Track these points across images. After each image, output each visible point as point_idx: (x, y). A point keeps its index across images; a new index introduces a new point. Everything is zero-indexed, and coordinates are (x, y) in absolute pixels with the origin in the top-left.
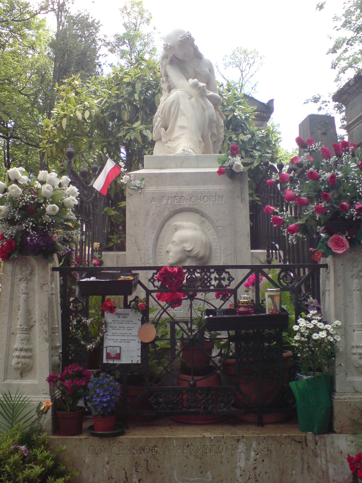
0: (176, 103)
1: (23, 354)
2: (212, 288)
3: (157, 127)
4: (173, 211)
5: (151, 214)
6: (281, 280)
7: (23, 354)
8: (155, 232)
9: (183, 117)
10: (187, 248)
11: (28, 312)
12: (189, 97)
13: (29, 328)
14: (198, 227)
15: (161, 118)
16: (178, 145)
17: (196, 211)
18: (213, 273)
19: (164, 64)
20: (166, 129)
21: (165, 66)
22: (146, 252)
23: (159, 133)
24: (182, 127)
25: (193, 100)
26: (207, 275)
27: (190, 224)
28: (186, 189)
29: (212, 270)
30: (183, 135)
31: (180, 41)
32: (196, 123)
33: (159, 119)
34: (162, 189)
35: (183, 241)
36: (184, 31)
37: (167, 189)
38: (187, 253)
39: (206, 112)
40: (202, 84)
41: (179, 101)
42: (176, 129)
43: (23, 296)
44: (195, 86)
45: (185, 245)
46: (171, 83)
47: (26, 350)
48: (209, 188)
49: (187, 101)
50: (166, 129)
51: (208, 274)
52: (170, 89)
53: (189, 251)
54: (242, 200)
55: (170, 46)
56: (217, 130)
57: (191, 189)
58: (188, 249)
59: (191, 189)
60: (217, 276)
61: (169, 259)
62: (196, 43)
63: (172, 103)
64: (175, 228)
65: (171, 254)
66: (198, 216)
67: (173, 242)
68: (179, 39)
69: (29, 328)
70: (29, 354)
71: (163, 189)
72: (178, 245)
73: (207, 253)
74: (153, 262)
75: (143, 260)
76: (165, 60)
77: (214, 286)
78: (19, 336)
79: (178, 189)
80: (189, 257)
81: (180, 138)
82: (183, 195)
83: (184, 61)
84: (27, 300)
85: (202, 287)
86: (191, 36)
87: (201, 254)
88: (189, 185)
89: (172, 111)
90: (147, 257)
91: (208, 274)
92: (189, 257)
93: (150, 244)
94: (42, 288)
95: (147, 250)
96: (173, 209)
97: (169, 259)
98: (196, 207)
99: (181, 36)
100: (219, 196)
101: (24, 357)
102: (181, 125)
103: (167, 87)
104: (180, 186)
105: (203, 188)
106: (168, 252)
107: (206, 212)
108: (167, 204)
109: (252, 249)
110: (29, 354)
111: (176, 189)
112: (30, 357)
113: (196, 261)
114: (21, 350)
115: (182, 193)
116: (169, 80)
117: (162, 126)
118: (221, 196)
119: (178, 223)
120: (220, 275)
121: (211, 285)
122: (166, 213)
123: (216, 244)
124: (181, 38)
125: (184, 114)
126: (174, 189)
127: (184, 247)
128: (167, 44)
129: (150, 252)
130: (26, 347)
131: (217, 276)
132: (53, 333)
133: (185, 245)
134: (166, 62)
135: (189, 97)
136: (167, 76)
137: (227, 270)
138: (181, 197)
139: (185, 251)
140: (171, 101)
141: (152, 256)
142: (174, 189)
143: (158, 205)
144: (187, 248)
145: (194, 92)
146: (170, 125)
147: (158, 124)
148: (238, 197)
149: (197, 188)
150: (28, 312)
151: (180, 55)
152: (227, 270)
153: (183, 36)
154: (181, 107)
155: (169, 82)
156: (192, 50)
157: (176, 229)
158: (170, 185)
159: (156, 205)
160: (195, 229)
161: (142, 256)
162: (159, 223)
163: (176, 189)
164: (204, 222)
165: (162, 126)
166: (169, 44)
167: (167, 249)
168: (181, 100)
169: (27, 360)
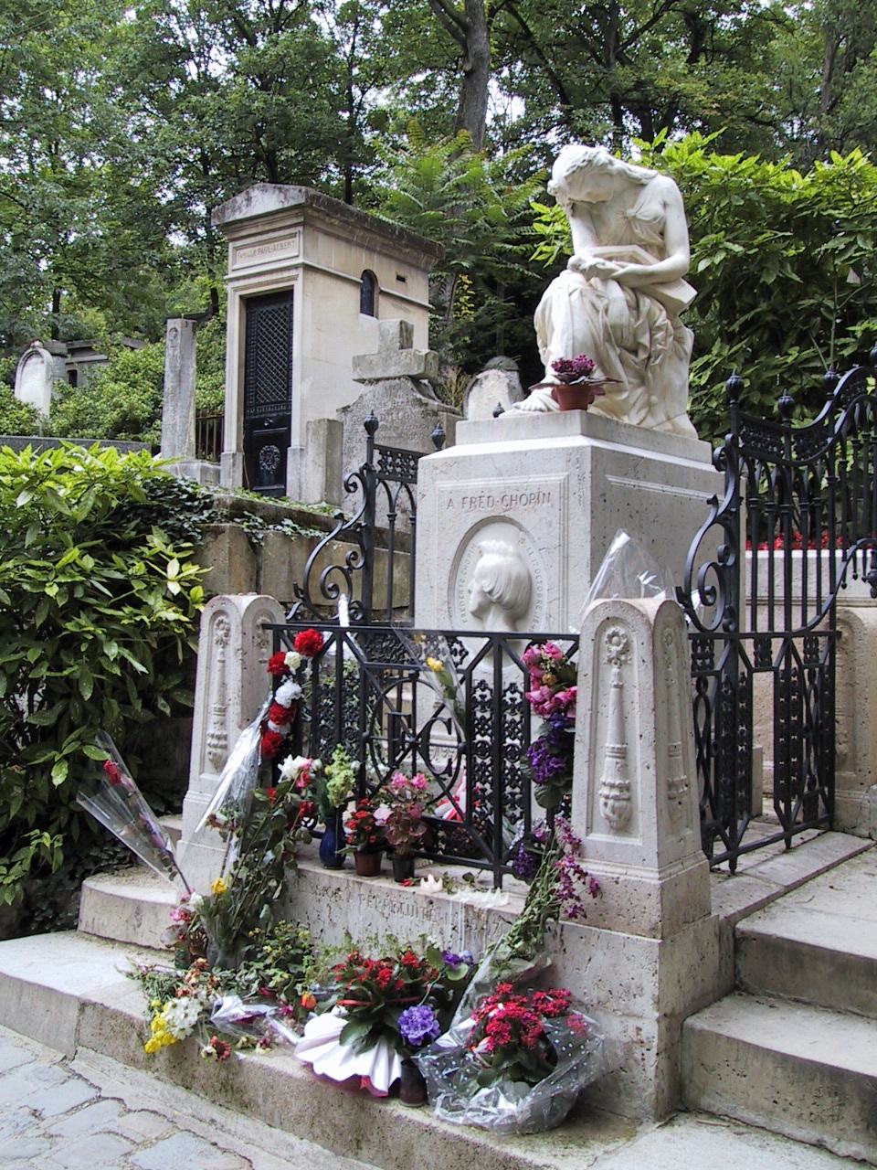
1: (215, 742)
7: (215, 742)
11: (223, 685)
13: (223, 711)
14: (511, 549)
17: (511, 521)
27: (501, 544)
32: (571, 342)
34: (463, 484)
35: (482, 576)
43: (219, 665)
47: (219, 738)
53: (490, 592)
56: (651, 337)
58: (487, 590)
65: (472, 596)
66: (515, 529)
69: (223, 711)
70: (222, 742)
78: (214, 718)
80: (492, 602)
84: (223, 670)
87: (507, 598)
88: (502, 475)
98: (509, 514)
101: (215, 746)
106: (470, 592)
107: (524, 524)
110: (222, 742)
112: (225, 747)
114: (213, 736)
123: (539, 580)
130: (218, 733)
133: (484, 581)
137: (459, 639)
150: (223, 685)
152: (459, 639)
157: (481, 554)
158: (477, 477)
160: (505, 553)
167: (469, 587)
169: (219, 751)
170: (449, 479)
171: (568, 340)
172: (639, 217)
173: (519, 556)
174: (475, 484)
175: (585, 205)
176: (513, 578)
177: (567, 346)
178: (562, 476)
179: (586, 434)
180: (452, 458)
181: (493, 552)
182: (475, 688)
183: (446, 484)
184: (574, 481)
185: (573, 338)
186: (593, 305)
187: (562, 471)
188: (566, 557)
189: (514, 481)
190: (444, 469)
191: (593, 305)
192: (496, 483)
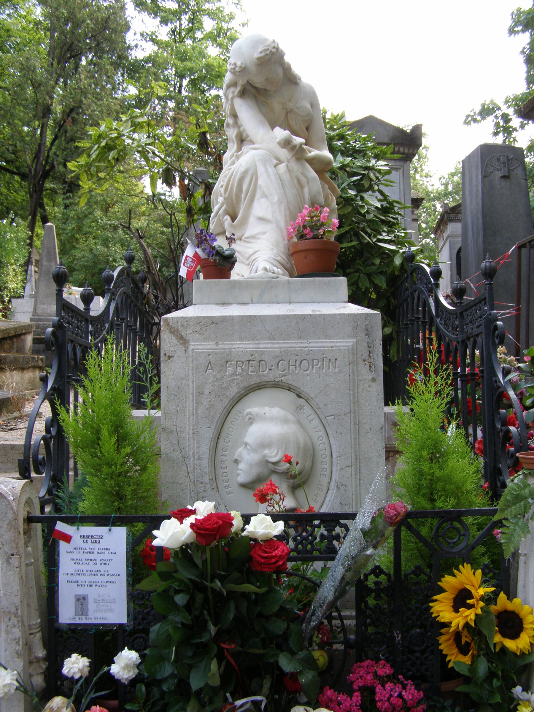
0: (250, 175)
2: (316, 553)
3: (217, 213)
4: (244, 388)
5: (206, 392)
6: (441, 538)
8: (213, 426)
9: (263, 200)
10: (271, 457)
12: (275, 162)
14: (290, 417)
15: (225, 199)
16: (255, 252)
18: (319, 526)
19: (230, 96)
20: (233, 219)
21: (232, 99)
22: (197, 462)
23: (221, 224)
24: (261, 219)
25: (282, 167)
26: (306, 531)
27: (276, 411)
28: (269, 346)
29: (316, 522)
30: (264, 233)
31: (258, 59)
32: (288, 212)
33: (221, 199)
34: (226, 345)
35: (263, 445)
36: (266, 40)
37: (234, 346)
38: (271, 466)
39: (306, 190)
40: (298, 140)
41: (256, 170)
42: (252, 220)
44: (286, 144)
45: (266, 452)
46: (242, 129)
48: (311, 345)
49: (271, 170)
50: (233, 219)
51: (309, 529)
52: (242, 140)
54: (370, 367)
55: (240, 67)
57: (278, 346)
58: (274, 460)
59: (278, 346)
60: (326, 533)
61: (238, 475)
62: (287, 59)
63: (245, 173)
64: (250, 418)
65: (242, 466)
66: (292, 396)
67: (246, 444)
68: (257, 55)
71: (227, 347)
72: (254, 450)
73: (308, 464)
74: (210, 479)
75: (192, 477)
76: (232, 89)
77: (319, 550)
79: (255, 346)
81: (259, 239)
82: (263, 358)
83: (266, 90)
85: (299, 552)
86: (277, 49)
88: (274, 339)
89: (245, 187)
90: (199, 471)
91: (309, 529)
92: (274, 472)
93: (205, 448)
94: (8, 561)
95: (199, 459)
96: (245, 384)
97: (238, 475)
99: (261, 49)
100: (330, 360)
102: (261, 215)
103: (236, 137)
104: (258, 340)
105: (301, 345)
106: (236, 462)
107: (306, 390)
108: (234, 374)
109: (386, 404)
111: (251, 346)
113: (288, 479)
115: (262, 353)
116: (239, 123)
117: (227, 213)
118: (333, 360)
119: (255, 410)
120: (330, 530)
121: (313, 549)
122: (234, 391)
124: (261, 53)
125: (265, 196)
126: (248, 346)
127: (265, 456)
128: (235, 64)
129: (205, 462)
131: (326, 533)
132: (31, 634)
133: (266, 452)
134: (233, 92)
135: (275, 162)
136: (235, 116)
137: (342, 522)
138: (260, 361)
139: (268, 462)
140: (242, 169)
141: (207, 470)
142: (248, 346)
143: (219, 376)
144: (271, 457)
145: (284, 153)
146: (241, 211)
147: (220, 209)
148: (364, 361)
149: (289, 345)
151: (258, 81)
153: (265, 50)
154: (260, 182)
155: (239, 127)
156: (280, 71)
157: (251, 420)
158: (241, 339)
159: (215, 377)
160: (285, 421)
161: (191, 469)
162: (220, 408)
163: (251, 346)
164: (301, 407)
165: (227, 213)
166: (239, 64)
167: (236, 457)
168: (261, 170)
170: (206, 339)
171: (285, 210)
172: (295, 110)
173: (300, 424)
174: (242, 346)
175: (253, 90)
176: (302, 446)
177: (286, 216)
178: (350, 342)
179: (353, 299)
180: (209, 317)
181: (272, 419)
182: (366, 576)
183: (200, 346)
184: (363, 349)
185: (289, 209)
186: (299, 181)
187: (349, 337)
188: (357, 424)
189: (295, 344)
190: (198, 328)
191: (299, 181)
192: (270, 347)
